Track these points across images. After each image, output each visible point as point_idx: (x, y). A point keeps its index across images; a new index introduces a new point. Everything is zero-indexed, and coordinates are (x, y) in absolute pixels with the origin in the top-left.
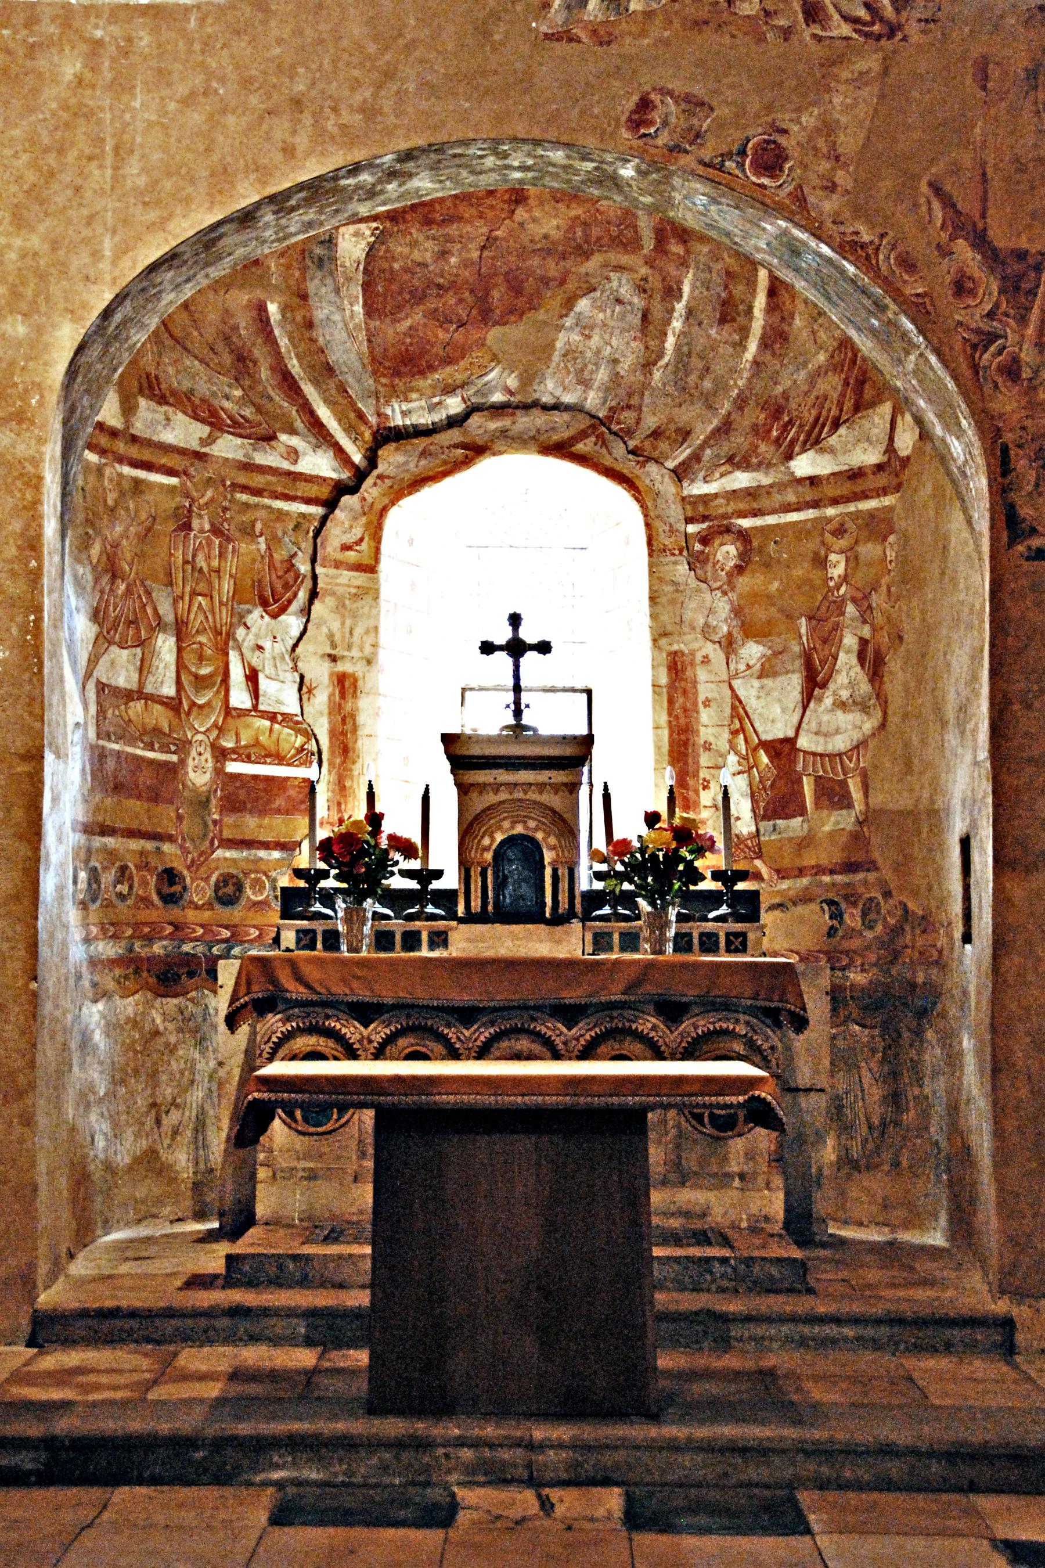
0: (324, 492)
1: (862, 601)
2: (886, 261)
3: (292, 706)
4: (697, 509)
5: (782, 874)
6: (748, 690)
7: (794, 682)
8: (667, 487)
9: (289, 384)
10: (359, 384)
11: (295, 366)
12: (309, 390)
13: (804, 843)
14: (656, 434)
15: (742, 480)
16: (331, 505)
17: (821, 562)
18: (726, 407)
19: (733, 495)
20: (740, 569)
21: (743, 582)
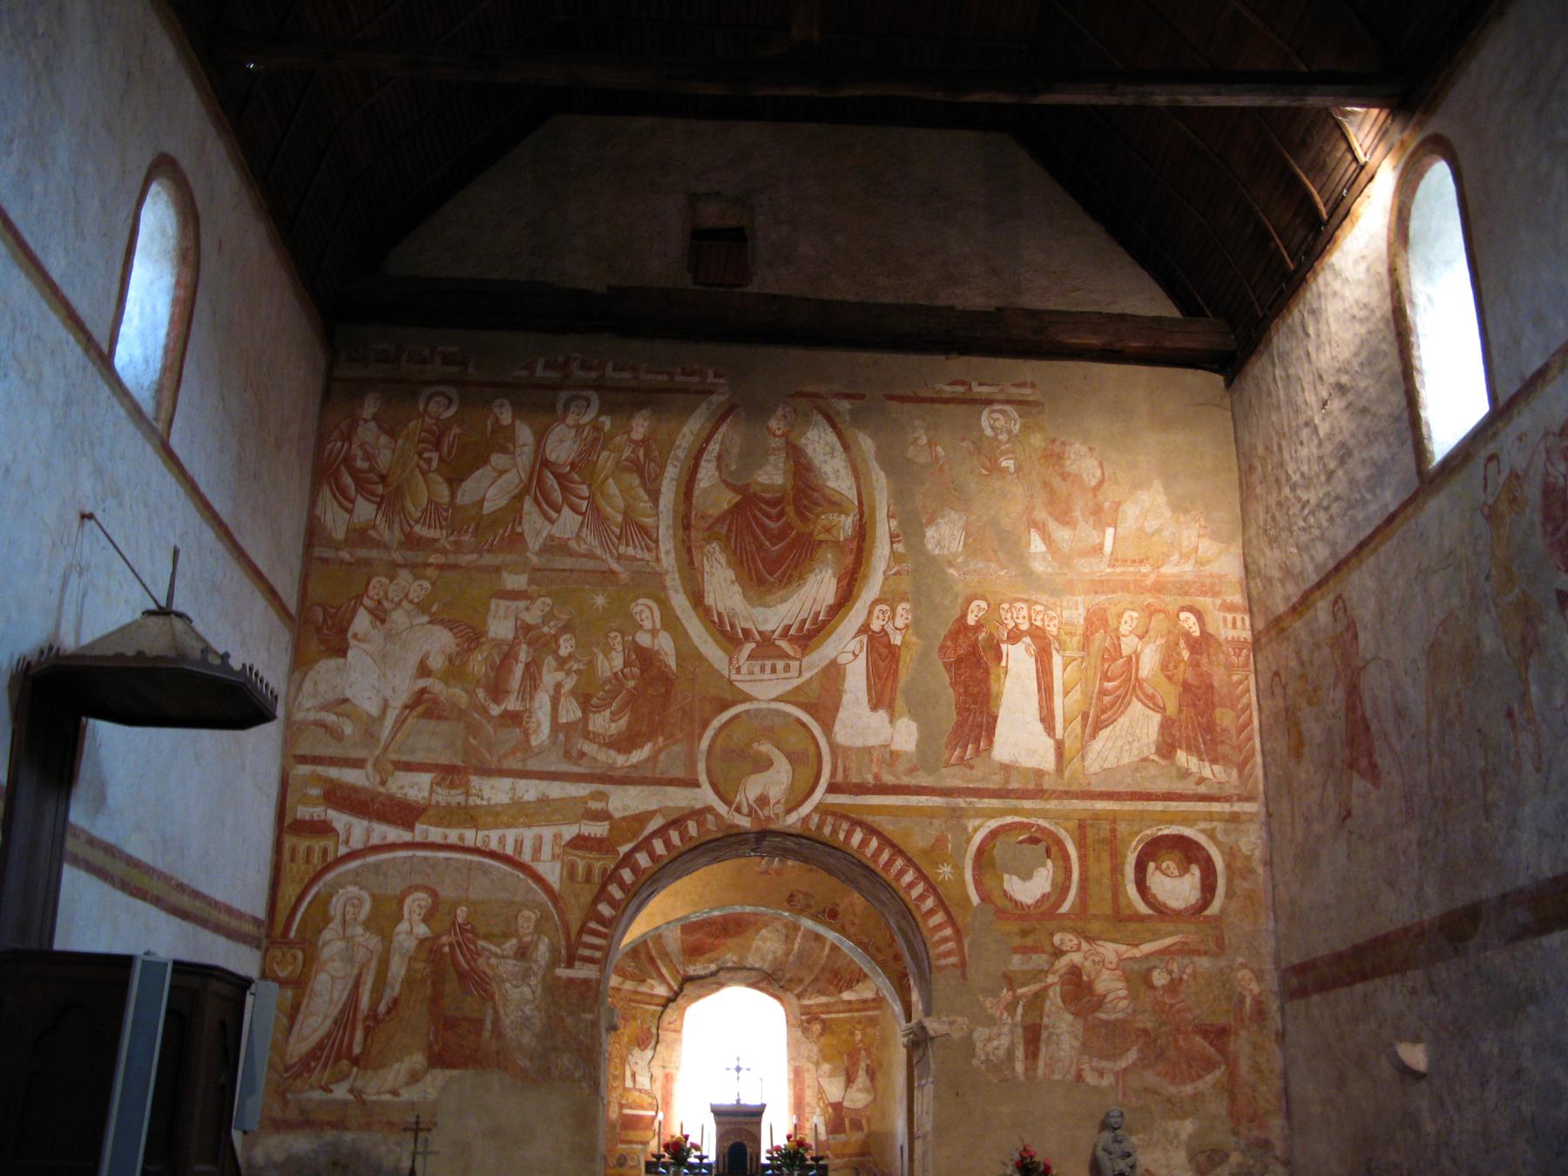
0: (663, 1001)
1: (868, 1050)
2: (872, 949)
3: (647, 1086)
4: (806, 1010)
5: (837, 1156)
6: (825, 1082)
7: (841, 1081)
8: (794, 1001)
9: (652, 960)
10: (677, 959)
11: (654, 953)
12: (659, 962)
13: (846, 1144)
14: (790, 980)
15: (823, 999)
16: (665, 1006)
17: (852, 1034)
18: (817, 971)
19: (819, 1005)
20: (822, 1034)
21: (823, 1040)
